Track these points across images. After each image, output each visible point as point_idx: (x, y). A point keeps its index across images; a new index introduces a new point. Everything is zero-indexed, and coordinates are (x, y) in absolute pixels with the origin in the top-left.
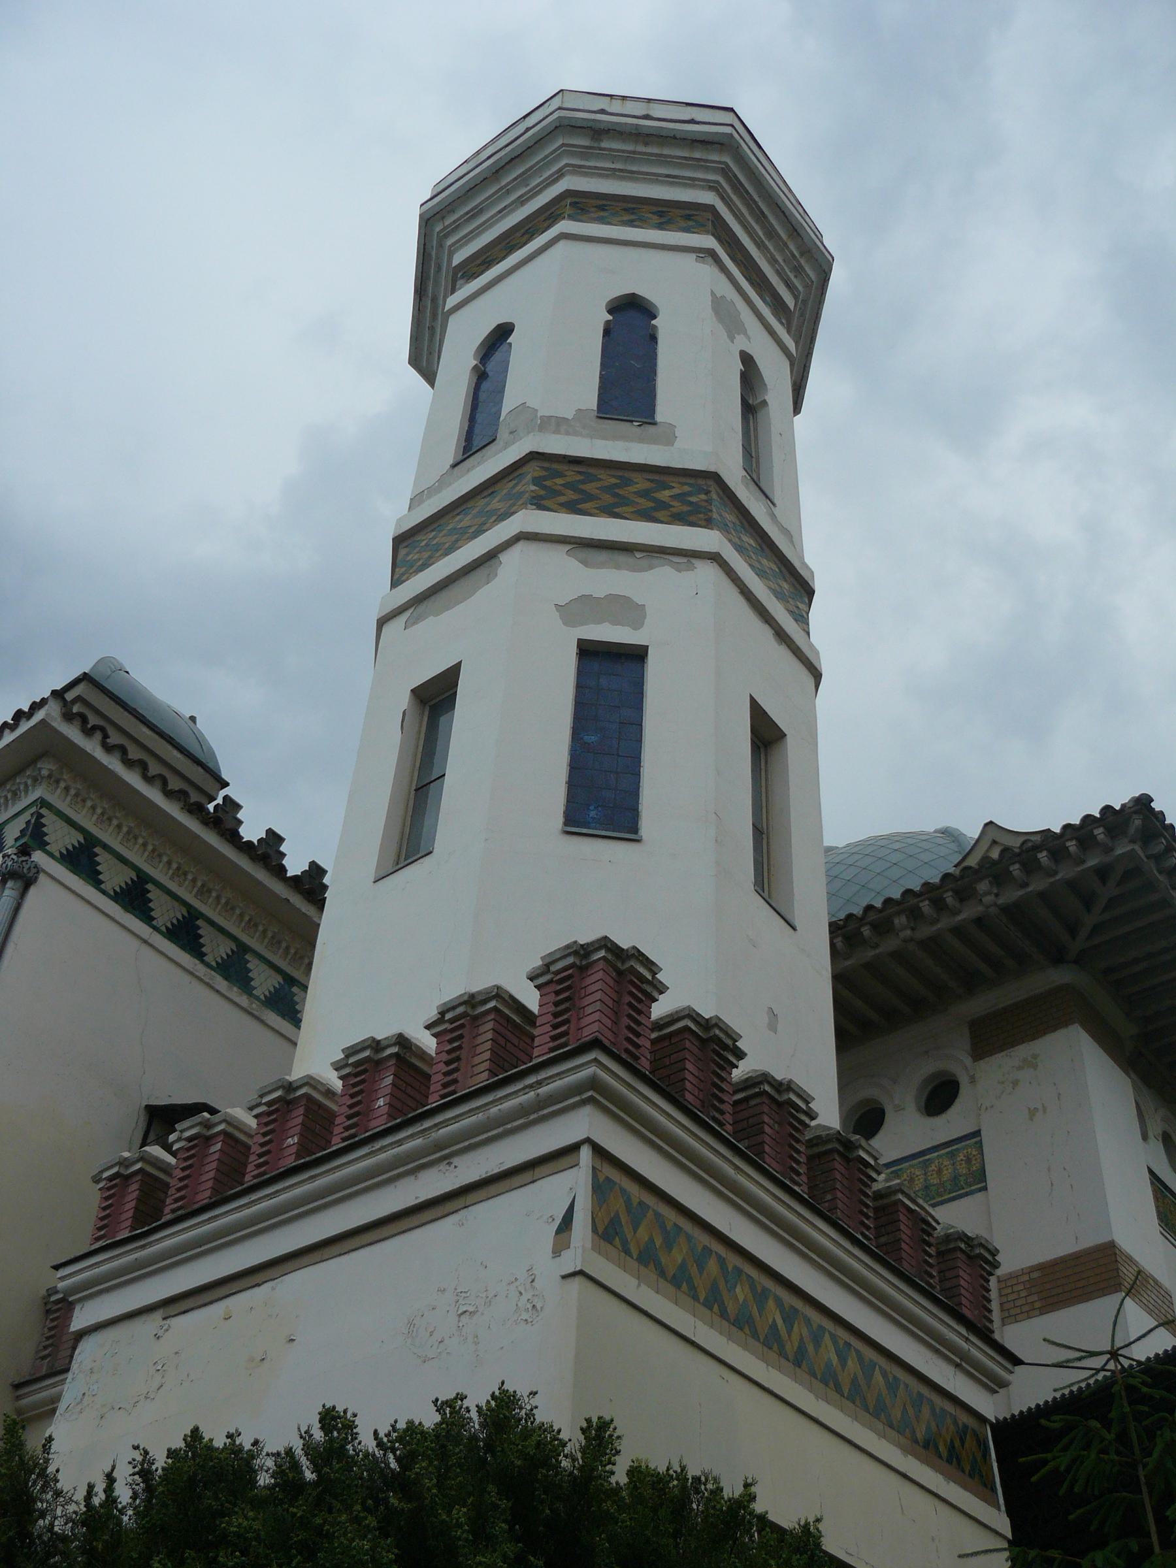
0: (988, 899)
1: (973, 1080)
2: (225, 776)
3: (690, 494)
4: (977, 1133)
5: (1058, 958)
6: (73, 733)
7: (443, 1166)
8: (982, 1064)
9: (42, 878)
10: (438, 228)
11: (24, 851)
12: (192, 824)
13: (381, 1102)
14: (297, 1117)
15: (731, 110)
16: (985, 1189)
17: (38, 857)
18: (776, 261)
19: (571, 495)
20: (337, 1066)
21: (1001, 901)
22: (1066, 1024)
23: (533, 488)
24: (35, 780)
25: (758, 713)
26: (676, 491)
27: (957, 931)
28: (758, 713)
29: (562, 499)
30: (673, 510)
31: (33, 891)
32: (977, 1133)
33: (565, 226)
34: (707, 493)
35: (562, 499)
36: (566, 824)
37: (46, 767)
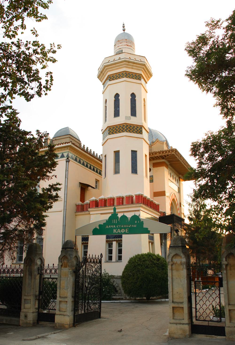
0: (158, 155)
1: (153, 170)
2: (81, 141)
3: (140, 129)
4: (153, 176)
5: (163, 158)
6: (72, 145)
7: (128, 209)
8: (154, 168)
9: (70, 161)
10: (106, 68)
11: (68, 158)
12: (80, 150)
13: (121, 201)
14: (112, 200)
15: (145, 57)
16: (153, 182)
17: (69, 159)
18: (146, 77)
19: (129, 129)
20: (116, 197)
21: (159, 155)
22: (163, 166)
23: (125, 128)
24: (67, 149)
25: (145, 154)
26: (139, 128)
27: (155, 157)
28: (145, 154)
29: (128, 130)
30: (139, 131)
31: (69, 162)
32: (153, 176)
33: (125, 79)
34: (142, 128)
35: (128, 130)
36: (132, 173)
37: (69, 148)
